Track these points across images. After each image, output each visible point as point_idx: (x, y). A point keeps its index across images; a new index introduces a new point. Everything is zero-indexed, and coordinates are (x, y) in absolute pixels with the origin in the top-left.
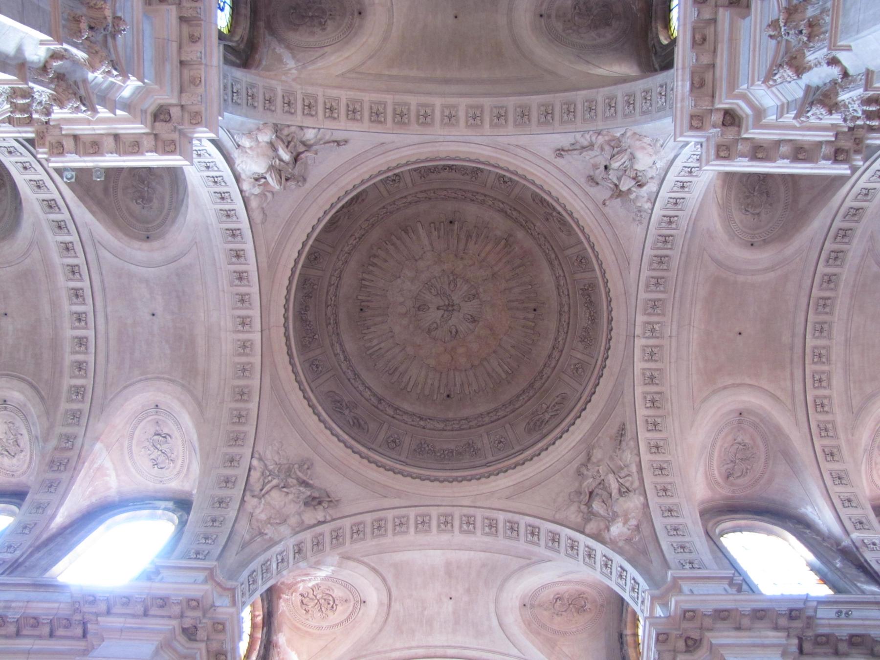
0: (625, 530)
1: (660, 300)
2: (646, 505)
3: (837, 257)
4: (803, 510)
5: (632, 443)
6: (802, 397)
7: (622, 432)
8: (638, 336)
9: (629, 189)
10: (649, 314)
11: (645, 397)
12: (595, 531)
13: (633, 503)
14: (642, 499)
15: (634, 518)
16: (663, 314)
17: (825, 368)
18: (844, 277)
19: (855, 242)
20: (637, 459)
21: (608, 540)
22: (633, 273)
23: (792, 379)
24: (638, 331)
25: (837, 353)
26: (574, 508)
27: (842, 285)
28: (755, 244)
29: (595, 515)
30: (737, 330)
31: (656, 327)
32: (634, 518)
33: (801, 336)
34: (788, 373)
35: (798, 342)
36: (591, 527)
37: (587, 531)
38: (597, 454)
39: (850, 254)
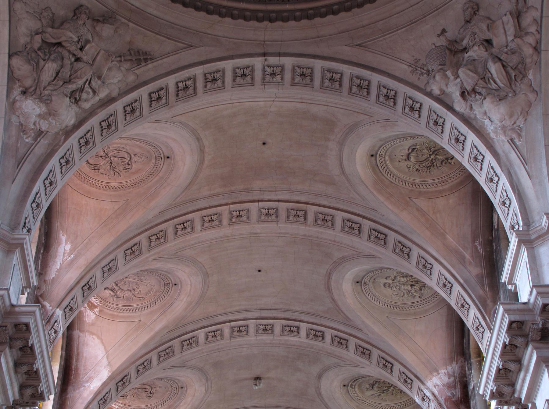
0: (33, 119)
1: (312, 80)
2: (68, 132)
3: (352, 227)
4: (64, 238)
5: (131, 78)
6: (190, 209)
7: (140, 57)
8: (266, 60)
9: (458, 76)
10: (294, 70)
11: (189, 79)
12: (17, 73)
13: (68, 115)
14: (72, 122)
15: (50, 124)
16: (293, 84)
17: (225, 222)
18: (330, 232)
19: (370, 245)
20: (115, 94)
21: (13, 97)
22: (347, 52)
23: (211, 196)
24: (273, 60)
25: (242, 229)
26: (35, 25)
27: (321, 230)
28: (373, 158)
29: (38, 69)
30: (269, 141)
31: (278, 78)
32: (50, 124)
33: (261, 197)
34: (218, 190)
35: (256, 197)
36: (22, 67)
37: (16, 61)
38: (107, 30)
39: (356, 239)
